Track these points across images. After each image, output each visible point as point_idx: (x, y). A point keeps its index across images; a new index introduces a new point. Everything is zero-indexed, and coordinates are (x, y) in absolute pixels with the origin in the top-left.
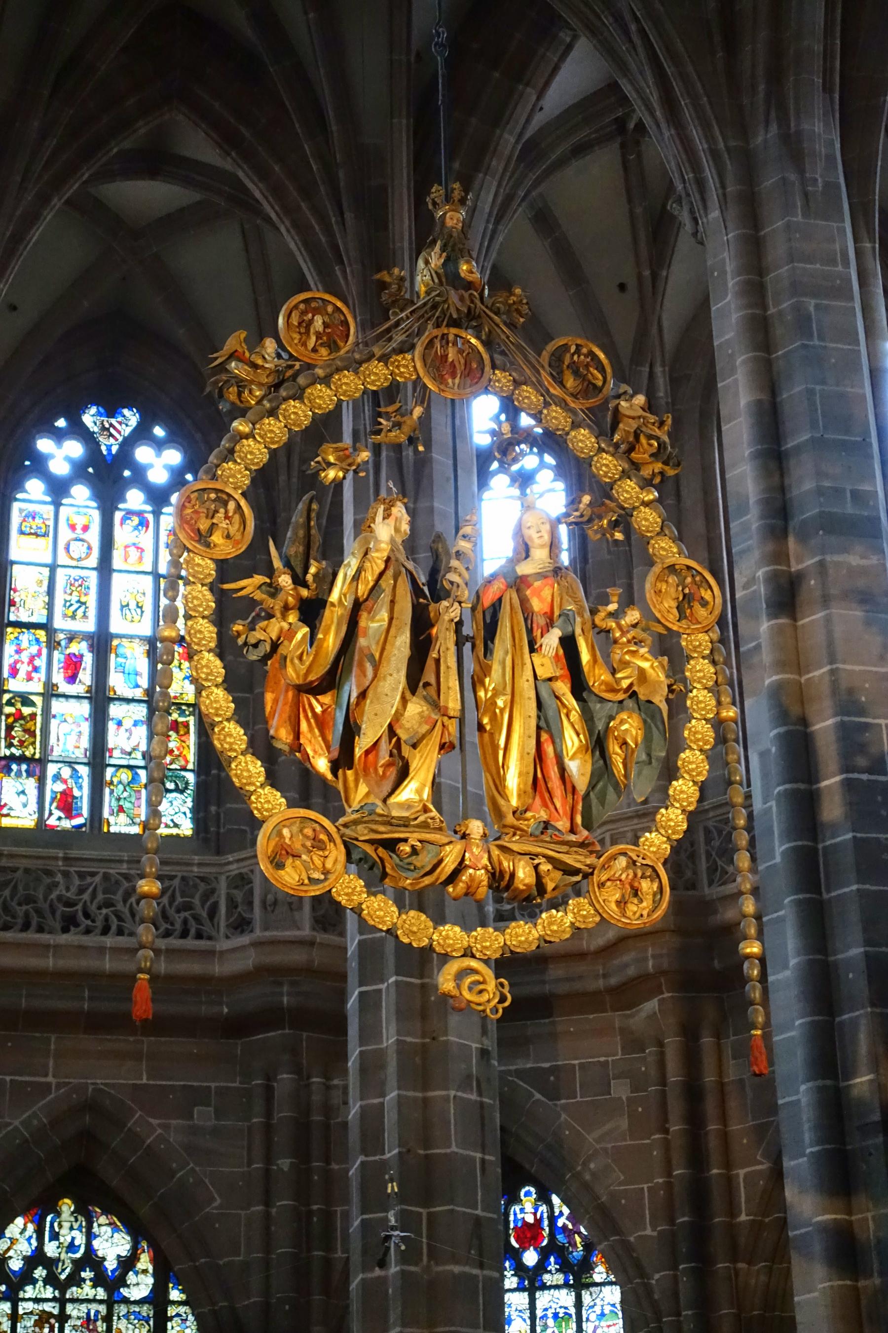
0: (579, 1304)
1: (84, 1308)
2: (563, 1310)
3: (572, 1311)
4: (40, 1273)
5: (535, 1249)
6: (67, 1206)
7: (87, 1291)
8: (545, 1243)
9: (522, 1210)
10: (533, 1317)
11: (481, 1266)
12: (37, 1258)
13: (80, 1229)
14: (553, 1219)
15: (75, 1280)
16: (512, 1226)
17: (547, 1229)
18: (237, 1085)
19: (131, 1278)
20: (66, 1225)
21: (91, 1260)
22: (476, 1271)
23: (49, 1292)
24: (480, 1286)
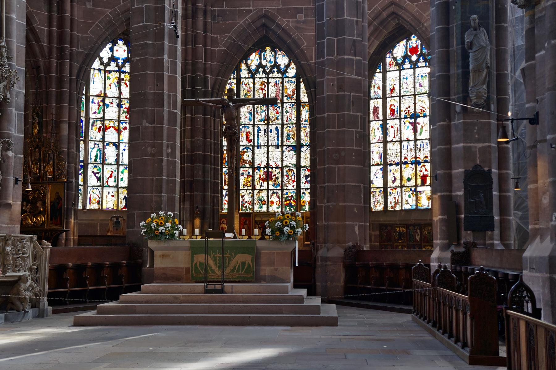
1: (275, 80)
4: (261, 70)
6: (268, 49)
7: (275, 74)
8: (419, 53)
10: (414, 77)
11: (355, 56)
12: (260, 65)
13: (273, 56)
15: (271, 71)
18: (311, 6)
19: (289, 70)
20: (268, 55)
21: (276, 65)
23: (264, 75)
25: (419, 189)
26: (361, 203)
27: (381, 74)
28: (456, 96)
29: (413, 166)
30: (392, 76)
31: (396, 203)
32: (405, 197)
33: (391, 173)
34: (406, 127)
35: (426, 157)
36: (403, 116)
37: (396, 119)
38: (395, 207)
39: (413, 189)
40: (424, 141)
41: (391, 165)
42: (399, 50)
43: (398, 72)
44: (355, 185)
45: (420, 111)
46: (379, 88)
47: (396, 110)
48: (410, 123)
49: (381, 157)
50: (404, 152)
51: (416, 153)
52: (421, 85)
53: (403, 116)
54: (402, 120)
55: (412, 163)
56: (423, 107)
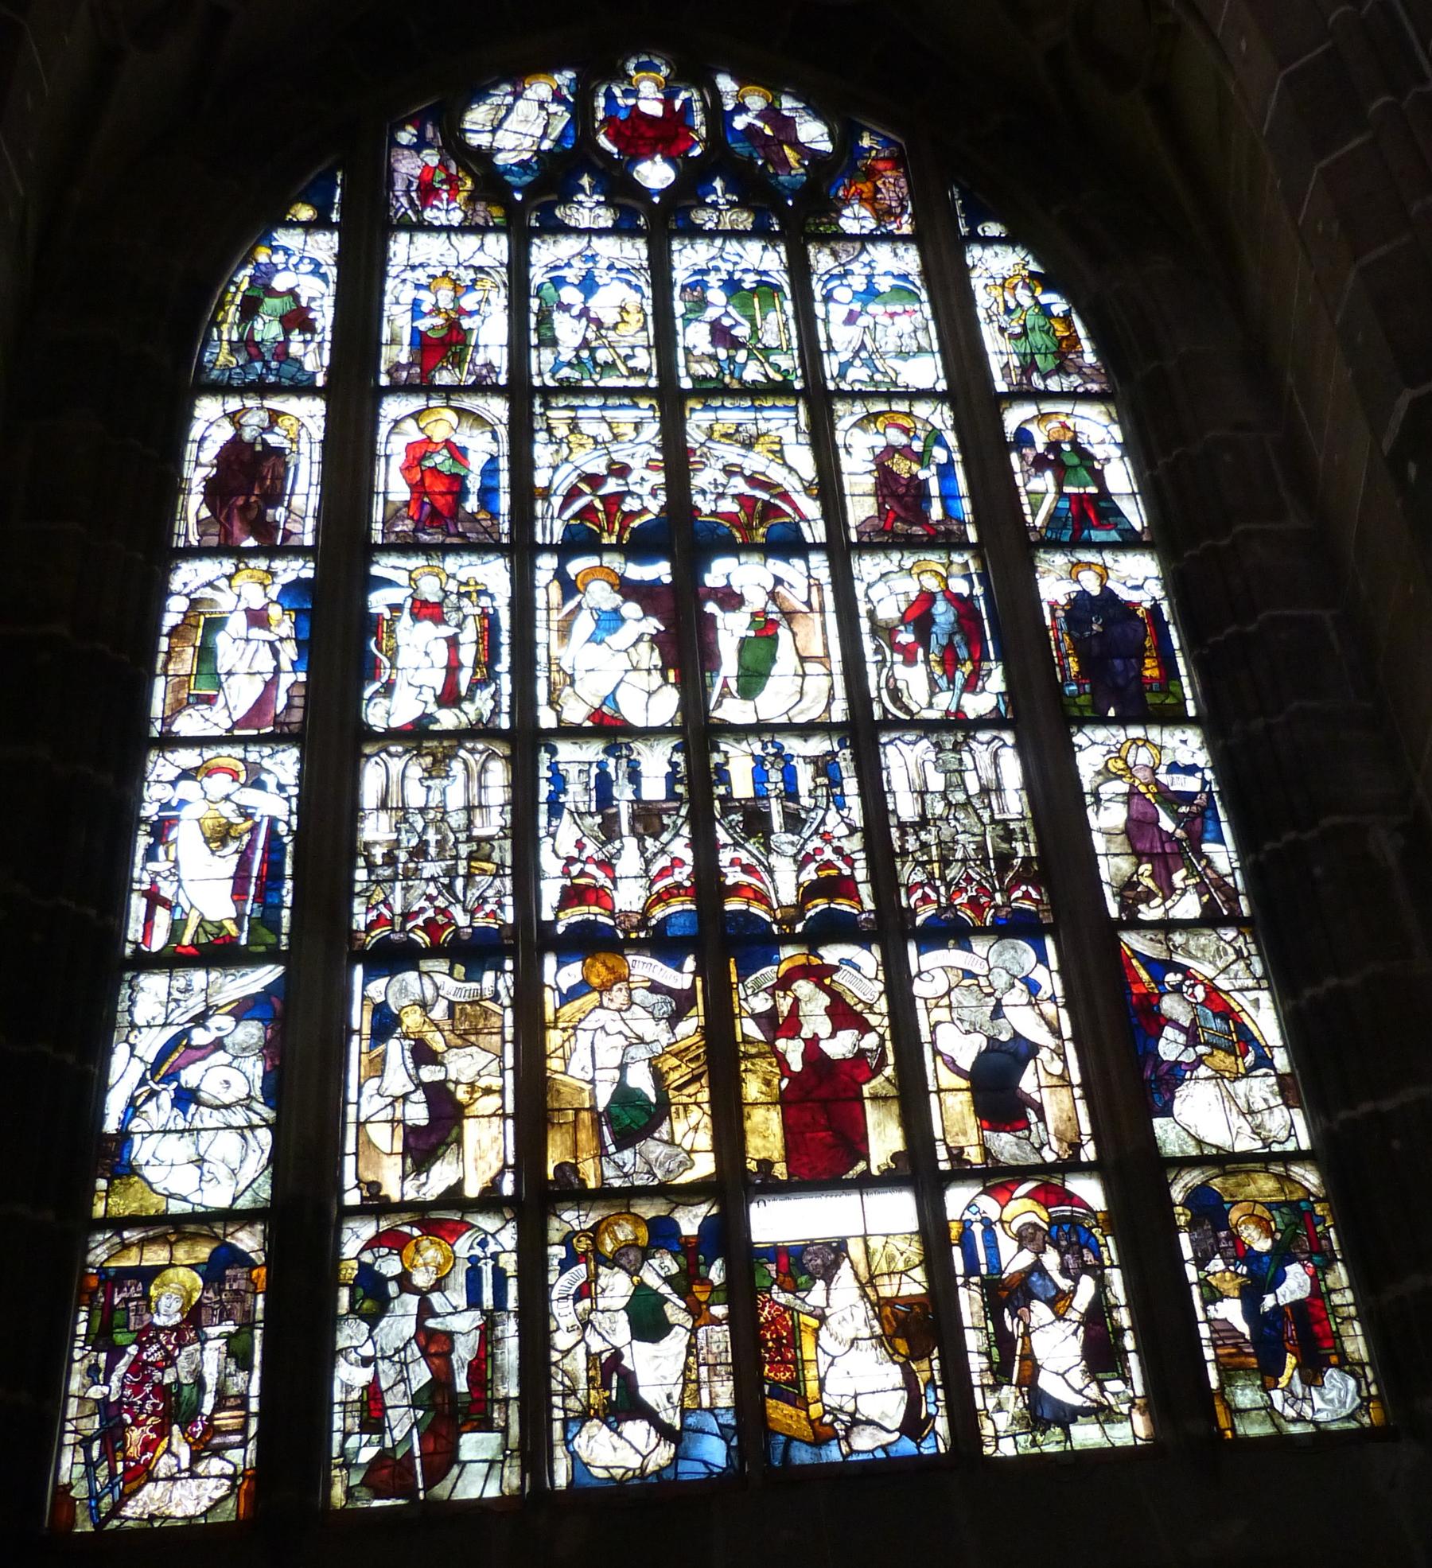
5: (669, 159)
14: (718, 117)
25: (773, 1222)
30: (438, 265)
31: (448, 1413)
32: (591, 1319)
33: (395, 1050)
35: (836, 886)
36: (551, 527)
39: (690, 1221)
40: (793, 745)
41: (393, 957)
45: (728, 506)
47: (474, 483)
48: (628, 589)
50: (562, 843)
51: (704, 846)
52: (720, 334)
53: (551, 527)
54: (546, 564)
55: (664, 944)
56: (752, 481)
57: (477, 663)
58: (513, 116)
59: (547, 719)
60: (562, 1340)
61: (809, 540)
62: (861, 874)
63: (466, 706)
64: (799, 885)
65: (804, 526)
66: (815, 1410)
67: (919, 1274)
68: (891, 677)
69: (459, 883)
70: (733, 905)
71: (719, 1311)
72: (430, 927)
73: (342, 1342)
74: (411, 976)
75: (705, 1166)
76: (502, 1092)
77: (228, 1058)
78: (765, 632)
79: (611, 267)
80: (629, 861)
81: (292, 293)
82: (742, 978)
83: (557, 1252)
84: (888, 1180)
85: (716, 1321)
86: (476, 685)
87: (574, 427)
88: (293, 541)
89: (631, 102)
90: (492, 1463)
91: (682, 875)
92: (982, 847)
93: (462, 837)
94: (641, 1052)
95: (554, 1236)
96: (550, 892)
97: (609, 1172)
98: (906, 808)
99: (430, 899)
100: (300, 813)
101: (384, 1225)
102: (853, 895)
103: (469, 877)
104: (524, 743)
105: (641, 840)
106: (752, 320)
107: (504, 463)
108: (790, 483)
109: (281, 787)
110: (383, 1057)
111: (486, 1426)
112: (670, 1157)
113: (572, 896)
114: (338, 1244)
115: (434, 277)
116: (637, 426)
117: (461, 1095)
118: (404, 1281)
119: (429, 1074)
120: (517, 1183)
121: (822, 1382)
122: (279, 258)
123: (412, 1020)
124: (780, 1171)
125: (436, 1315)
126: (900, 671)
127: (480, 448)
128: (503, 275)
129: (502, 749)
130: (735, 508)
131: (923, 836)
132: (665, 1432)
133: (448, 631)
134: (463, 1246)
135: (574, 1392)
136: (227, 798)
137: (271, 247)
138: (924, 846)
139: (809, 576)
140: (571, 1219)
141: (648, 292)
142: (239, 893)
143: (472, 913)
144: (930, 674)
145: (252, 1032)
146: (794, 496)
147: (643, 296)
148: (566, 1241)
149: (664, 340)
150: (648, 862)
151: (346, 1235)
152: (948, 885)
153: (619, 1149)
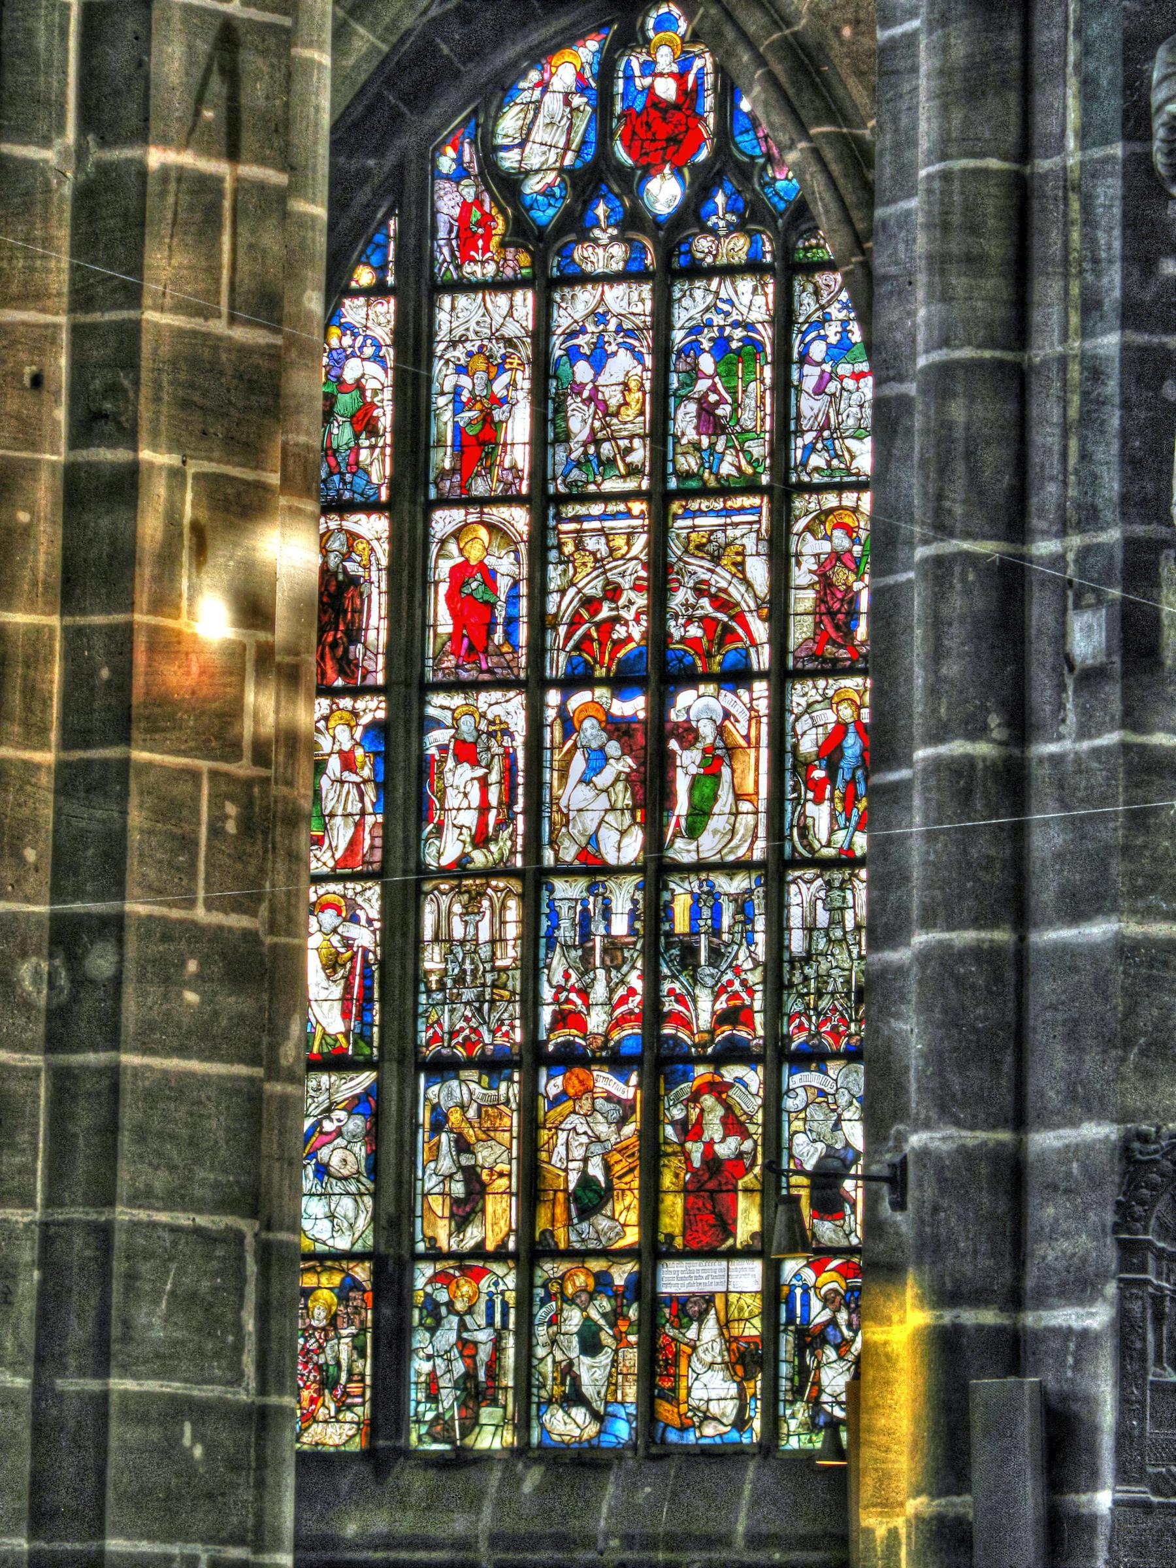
0: (784, 317)
2: (739, 333)
3: (766, 334)
5: (677, 172)
8: (703, 155)
9: (649, 68)
10: (663, 351)
11: (233, 154)
16: (618, 109)
17: (711, 119)
22: (218, 167)
24: (227, 204)
25: (677, 1278)
26: (237, 1379)
27: (386, 310)
28: (1076, 541)
29: (627, 1089)
31: (476, 1393)
34: (578, 764)
36: (558, 664)
37: (504, 685)
38: (471, 1424)
39: (621, 1274)
41: (443, 1068)
42: (542, 124)
43: (525, 302)
44: (198, 1231)
45: (695, 631)
46: (364, 422)
47: (500, 614)
49: (366, 1000)
51: (653, 978)
53: (558, 664)
54: (553, 697)
55: (618, 1062)
57: (500, 803)
58: (540, 121)
59: (549, 857)
60: (540, 1352)
61: (755, 667)
62: (758, 1005)
63: (493, 848)
64: (713, 1013)
65: (752, 650)
66: (683, 1408)
67: (757, 1322)
68: (803, 814)
69: (486, 1006)
70: (667, 1030)
71: (633, 1339)
72: (467, 1044)
73: (415, 1345)
74: (455, 1083)
75: (632, 1236)
76: (509, 1175)
77: (344, 1143)
78: (712, 768)
79: (619, 329)
80: (599, 992)
81: (359, 386)
82: (668, 1090)
83: (540, 1292)
84: (747, 1253)
85: (630, 1345)
86: (501, 824)
87: (579, 546)
88: (370, 681)
89: (647, 81)
90: (497, 1426)
91: (634, 1003)
92: (848, 981)
93: (488, 966)
94: (597, 1148)
95: (538, 1281)
96: (546, 1015)
97: (573, 1238)
98: (797, 942)
99: (467, 1020)
100: (383, 944)
101: (439, 1266)
102: (751, 1025)
103: (492, 1002)
104: (535, 881)
105: (608, 971)
106: (733, 391)
107: (523, 589)
108: (747, 602)
109: (370, 921)
110: (438, 1145)
111: (494, 1402)
112: (611, 1229)
113: (562, 1019)
114: (412, 1280)
115: (470, 354)
116: (630, 536)
117: (485, 1176)
118: (450, 1305)
119: (465, 1160)
120: (517, 1242)
121: (689, 1389)
122: (347, 341)
123: (455, 1117)
124: (679, 1242)
125: (467, 1330)
126: (810, 808)
127: (505, 566)
128: (526, 351)
129: (516, 886)
130: (699, 633)
131: (807, 970)
132: (596, 1416)
133: (480, 772)
134: (484, 1283)
135: (544, 1386)
136: (335, 931)
137: (340, 325)
138: (806, 979)
139: (751, 709)
140: (549, 1269)
141: (648, 361)
142: (346, 1015)
143: (493, 1032)
144: (833, 810)
145: (356, 1124)
146: (749, 618)
147: (645, 369)
148: (544, 1286)
149: (660, 433)
150: (612, 991)
151: (417, 1273)
152: (818, 1014)
153: (581, 1221)
